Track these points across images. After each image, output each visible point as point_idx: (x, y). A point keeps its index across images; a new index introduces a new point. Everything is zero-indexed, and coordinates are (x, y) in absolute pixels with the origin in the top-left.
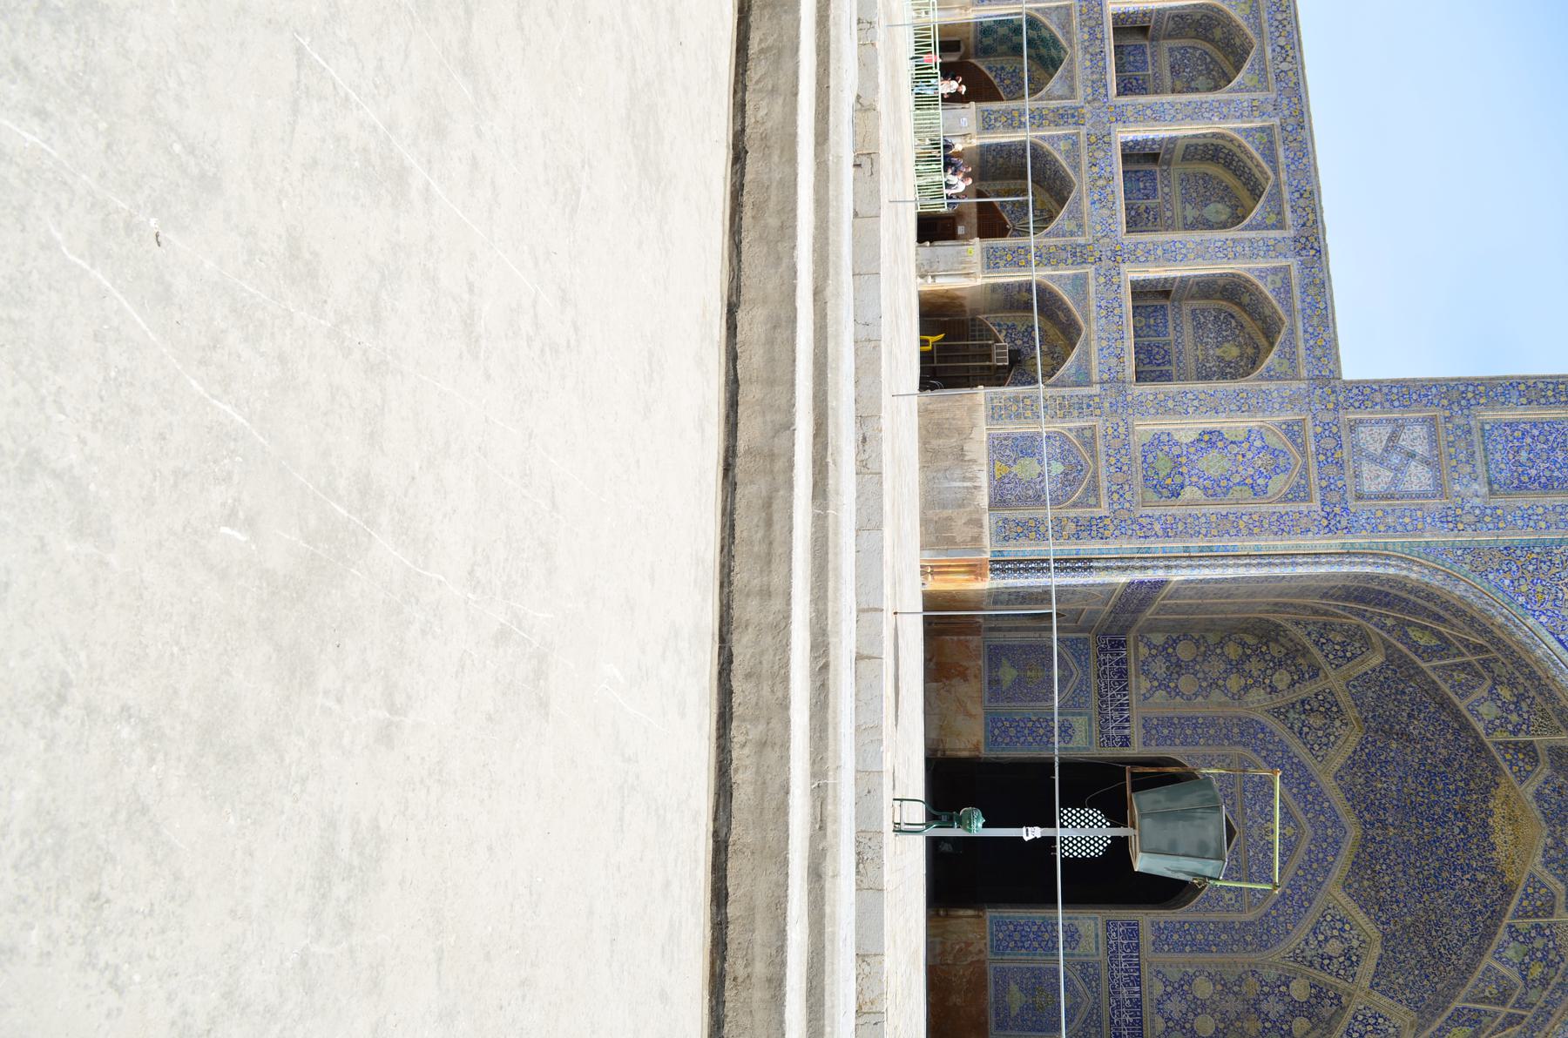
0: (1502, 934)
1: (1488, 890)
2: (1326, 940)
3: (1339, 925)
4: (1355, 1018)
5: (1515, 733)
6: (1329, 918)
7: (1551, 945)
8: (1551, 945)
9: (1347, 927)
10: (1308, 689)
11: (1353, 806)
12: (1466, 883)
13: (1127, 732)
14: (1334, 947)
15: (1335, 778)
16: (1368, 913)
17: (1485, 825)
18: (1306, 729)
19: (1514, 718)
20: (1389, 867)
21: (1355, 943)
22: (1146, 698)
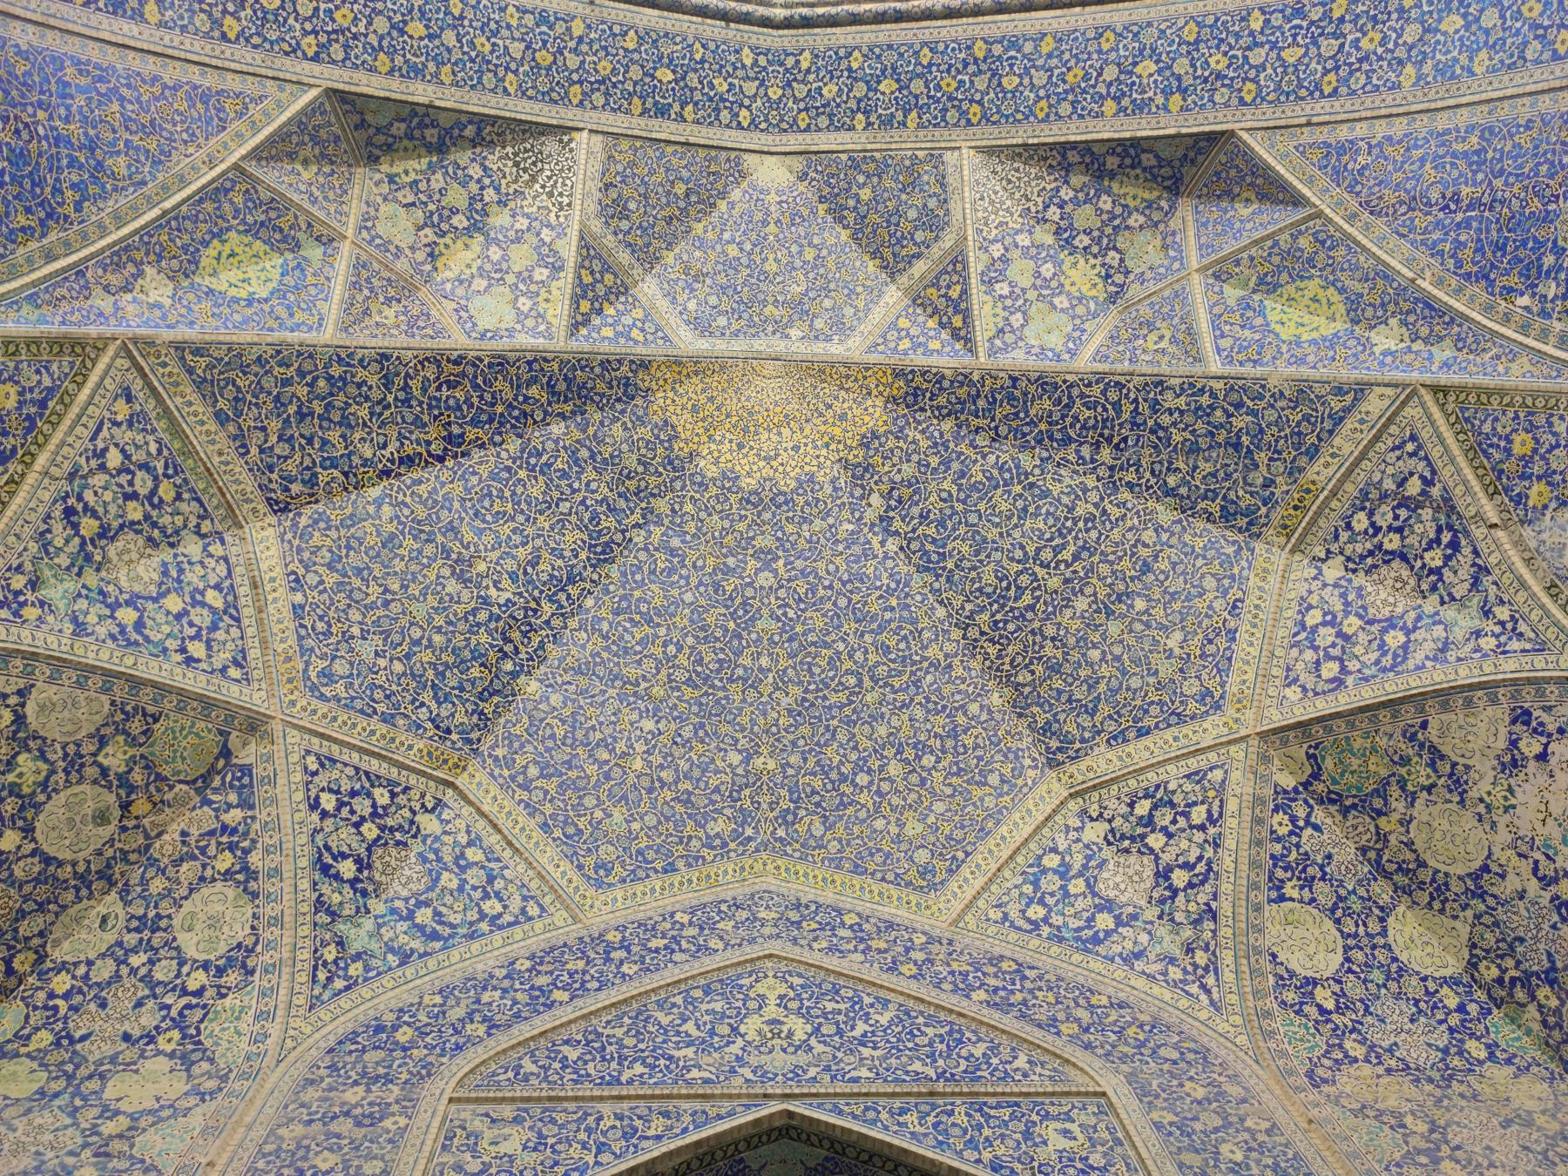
0: (1017, 359)
1: (908, 470)
2: (1108, 905)
3: (1051, 883)
4: (1338, 682)
5: (556, 269)
6: (1036, 912)
7: (1023, 240)
8: (1023, 240)
9: (1052, 861)
10: (285, 826)
11: (694, 860)
12: (892, 545)
14: (1128, 880)
15: (599, 884)
16: (997, 816)
17: (752, 500)
18: (424, 916)
19: (521, 256)
20: (860, 767)
21: (1094, 832)
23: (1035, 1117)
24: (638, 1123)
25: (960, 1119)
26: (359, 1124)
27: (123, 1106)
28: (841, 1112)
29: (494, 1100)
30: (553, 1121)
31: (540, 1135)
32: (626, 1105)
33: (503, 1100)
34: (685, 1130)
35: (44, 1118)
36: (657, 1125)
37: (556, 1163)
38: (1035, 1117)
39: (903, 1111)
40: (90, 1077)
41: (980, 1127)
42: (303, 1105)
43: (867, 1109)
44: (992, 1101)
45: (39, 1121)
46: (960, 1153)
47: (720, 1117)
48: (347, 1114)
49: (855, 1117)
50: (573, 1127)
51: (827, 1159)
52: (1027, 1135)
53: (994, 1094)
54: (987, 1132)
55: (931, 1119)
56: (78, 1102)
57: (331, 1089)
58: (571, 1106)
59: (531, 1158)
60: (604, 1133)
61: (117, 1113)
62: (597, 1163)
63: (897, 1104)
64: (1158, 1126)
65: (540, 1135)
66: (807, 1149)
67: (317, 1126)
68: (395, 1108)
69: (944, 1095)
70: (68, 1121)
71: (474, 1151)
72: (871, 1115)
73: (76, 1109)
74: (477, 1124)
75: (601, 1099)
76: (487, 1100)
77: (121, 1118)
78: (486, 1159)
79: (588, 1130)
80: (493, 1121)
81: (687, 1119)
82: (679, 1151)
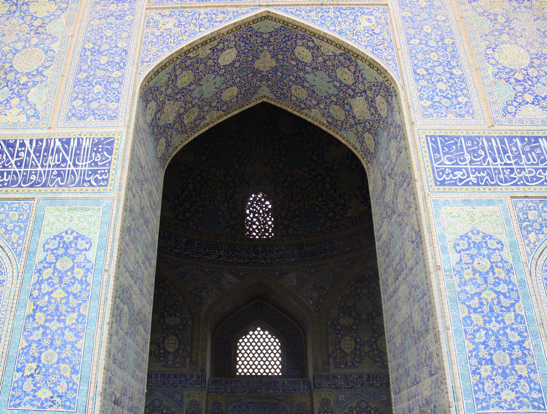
13: (86, 144)
22: (36, 115)
23: (359, 14)
24: (213, 16)
25: (331, 14)
26: (117, 19)
27: (37, 15)
28: (287, 12)
29: (162, 8)
30: (183, 16)
31: (179, 21)
32: (209, 9)
33: (165, 8)
34: (230, 19)
35: (14, 21)
36: (220, 17)
37: (186, 32)
38: (359, 14)
39: (310, 11)
40: (23, 4)
41: (338, 17)
42: (96, 13)
43: (297, 10)
44: (344, 7)
45: (12, 22)
46: (328, 27)
47: (243, 14)
48: (112, 15)
49: (292, 13)
50: (191, 18)
51: (282, 26)
52: (354, 20)
53: (345, 5)
54: (340, 19)
55: (320, 14)
56: (23, 15)
57: (105, 6)
58: (189, 10)
59: (176, 30)
60: (201, 20)
61: (37, 18)
62: (200, 31)
63: (309, 8)
64: (403, 18)
65: (179, 21)
66: (275, 23)
67: (103, 20)
68: (128, 12)
69: (326, 5)
70: (22, 22)
71: (157, 27)
72: (298, 12)
73: (23, 17)
74: (157, 17)
75: (200, 7)
76: (159, 8)
77: (38, 19)
78: (162, 30)
79: (196, 19)
80: (162, 16)
81: (231, 14)
82: (228, 26)
